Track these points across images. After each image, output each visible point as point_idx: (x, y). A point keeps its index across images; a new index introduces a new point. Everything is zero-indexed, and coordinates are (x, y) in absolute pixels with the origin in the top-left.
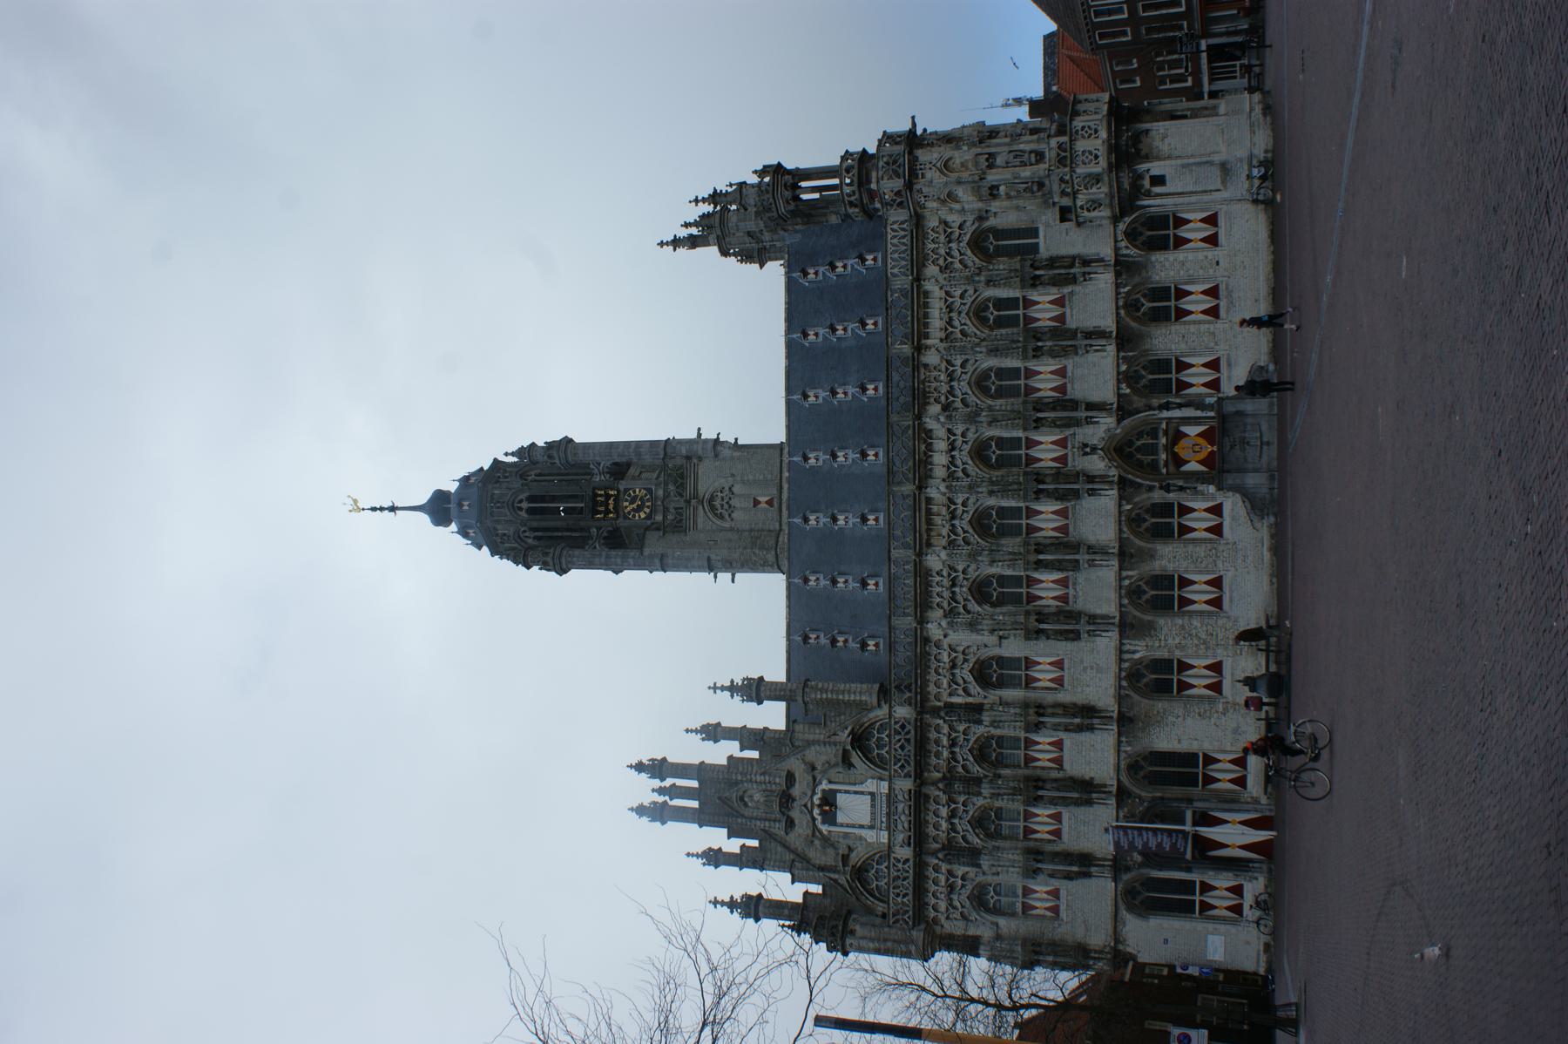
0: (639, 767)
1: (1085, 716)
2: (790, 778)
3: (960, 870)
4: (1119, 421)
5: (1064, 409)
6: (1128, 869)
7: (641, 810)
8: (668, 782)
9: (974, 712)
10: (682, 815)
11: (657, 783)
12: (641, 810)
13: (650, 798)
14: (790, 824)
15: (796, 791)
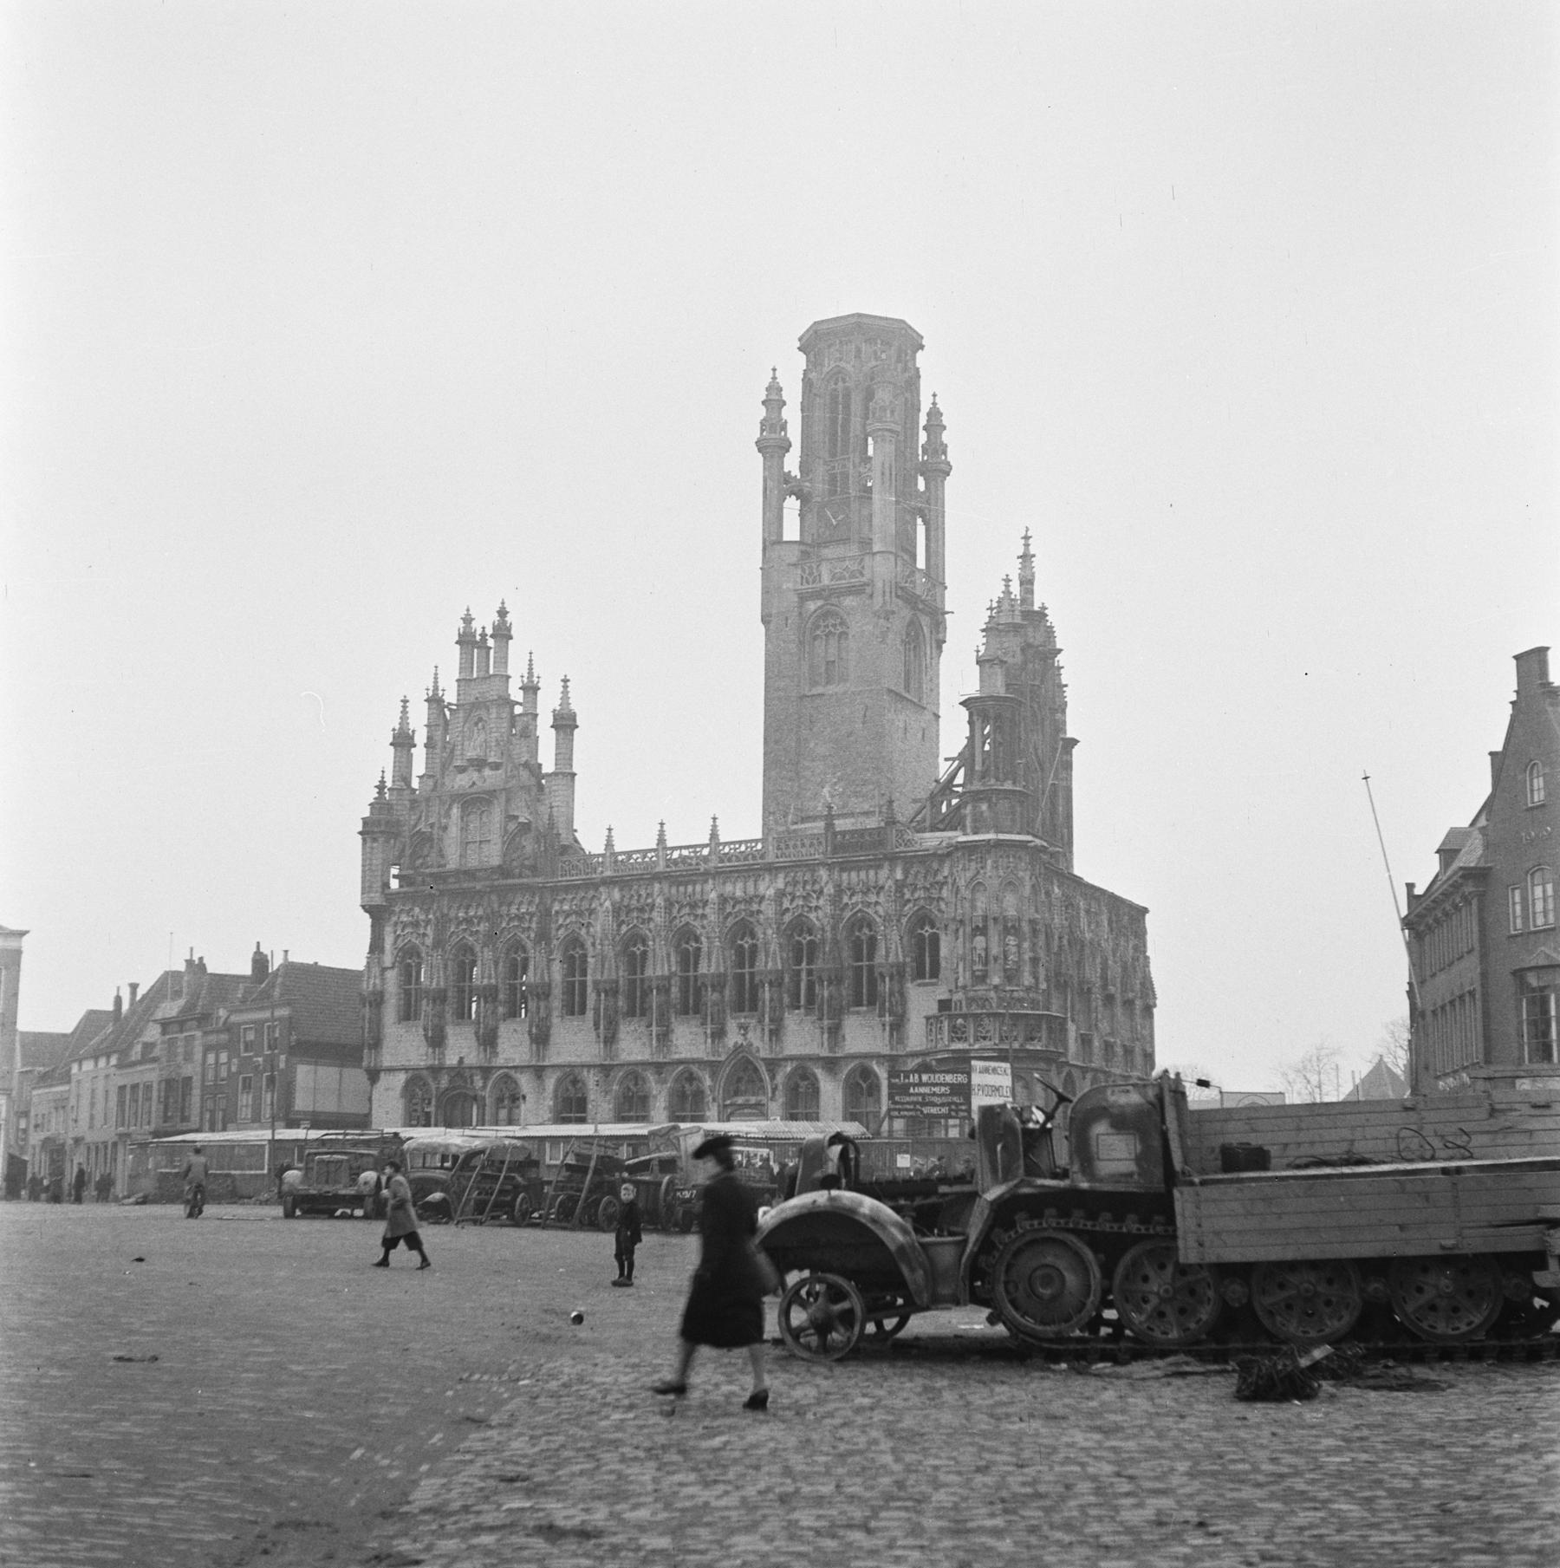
0: (503, 613)
1: (541, 1039)
2: (496, 766)
3: (430, 931)
4: (764, 1060)
5: (773, 1009)
6: (435, 1079)
7: (468, 620)
8: (491, 642)
9: (543, 936)
10: (466, 665)
11: (489, 631)
12: (468, 620)
13: (477, 626)
14: (462, 770)
15: (487, 772)
